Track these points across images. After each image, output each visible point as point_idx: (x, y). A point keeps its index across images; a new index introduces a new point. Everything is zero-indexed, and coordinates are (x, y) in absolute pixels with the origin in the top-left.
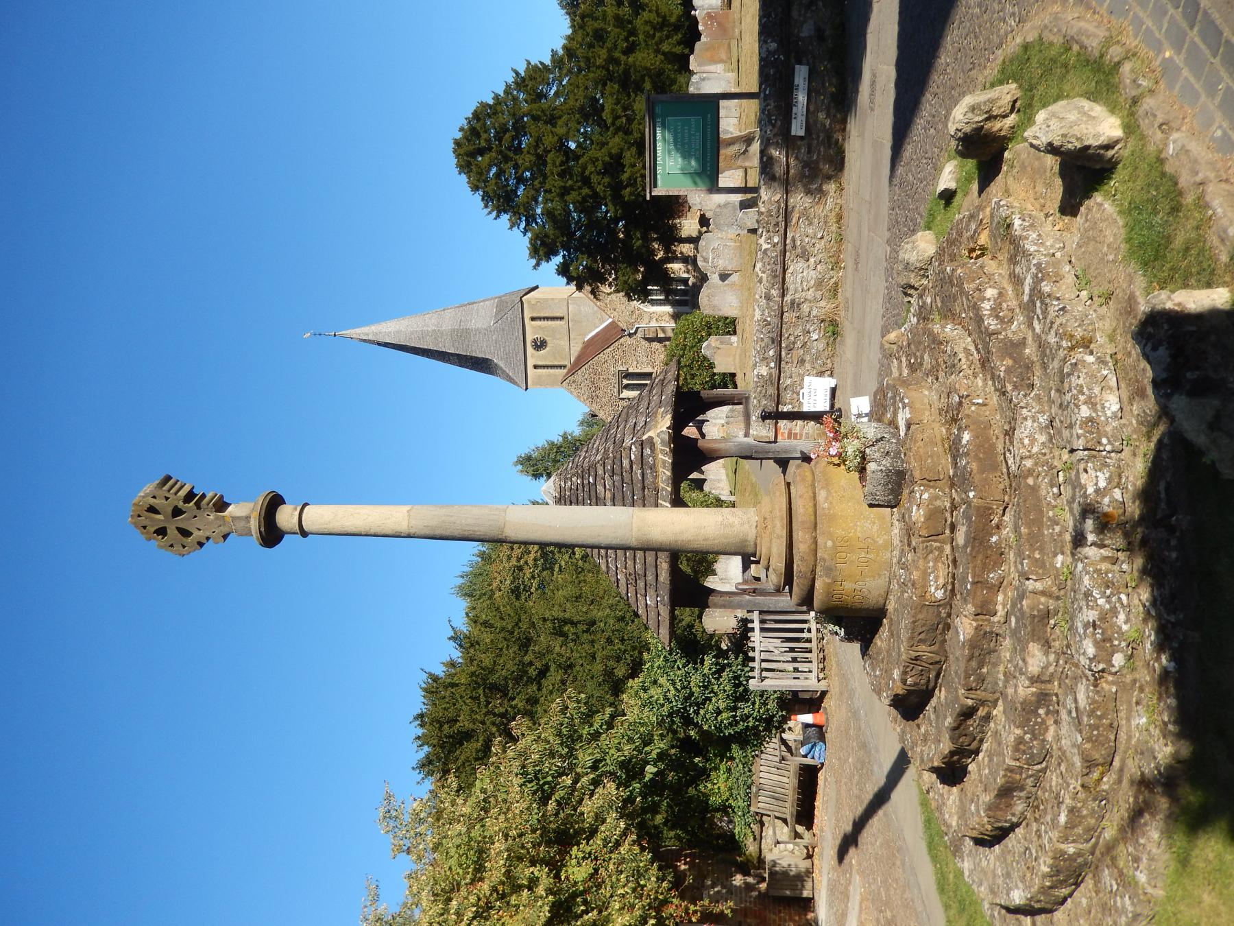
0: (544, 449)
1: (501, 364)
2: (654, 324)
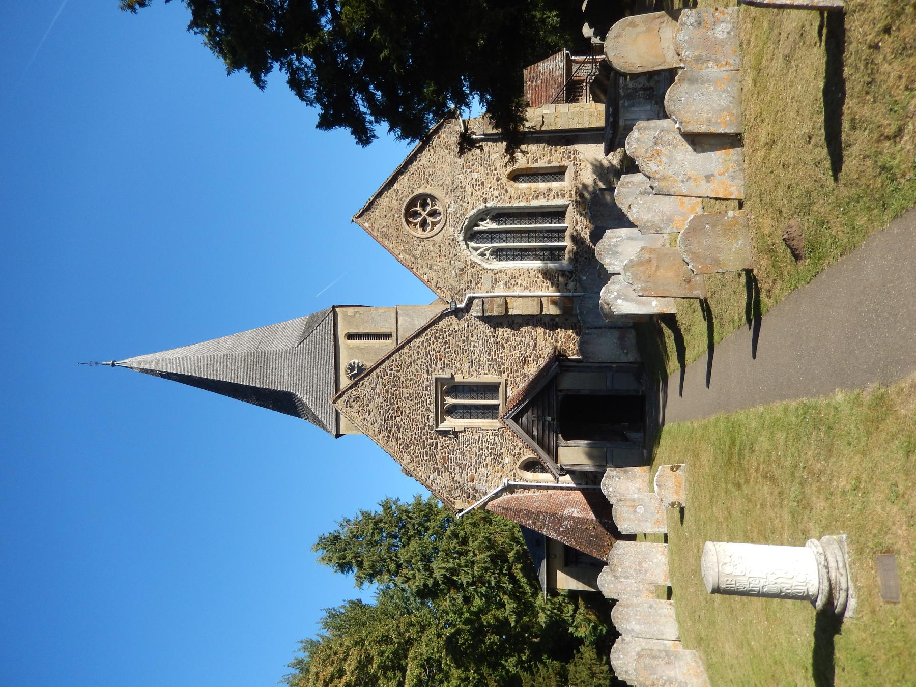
0: (357, 523)
1: (306, 400)
2: (500, 291)
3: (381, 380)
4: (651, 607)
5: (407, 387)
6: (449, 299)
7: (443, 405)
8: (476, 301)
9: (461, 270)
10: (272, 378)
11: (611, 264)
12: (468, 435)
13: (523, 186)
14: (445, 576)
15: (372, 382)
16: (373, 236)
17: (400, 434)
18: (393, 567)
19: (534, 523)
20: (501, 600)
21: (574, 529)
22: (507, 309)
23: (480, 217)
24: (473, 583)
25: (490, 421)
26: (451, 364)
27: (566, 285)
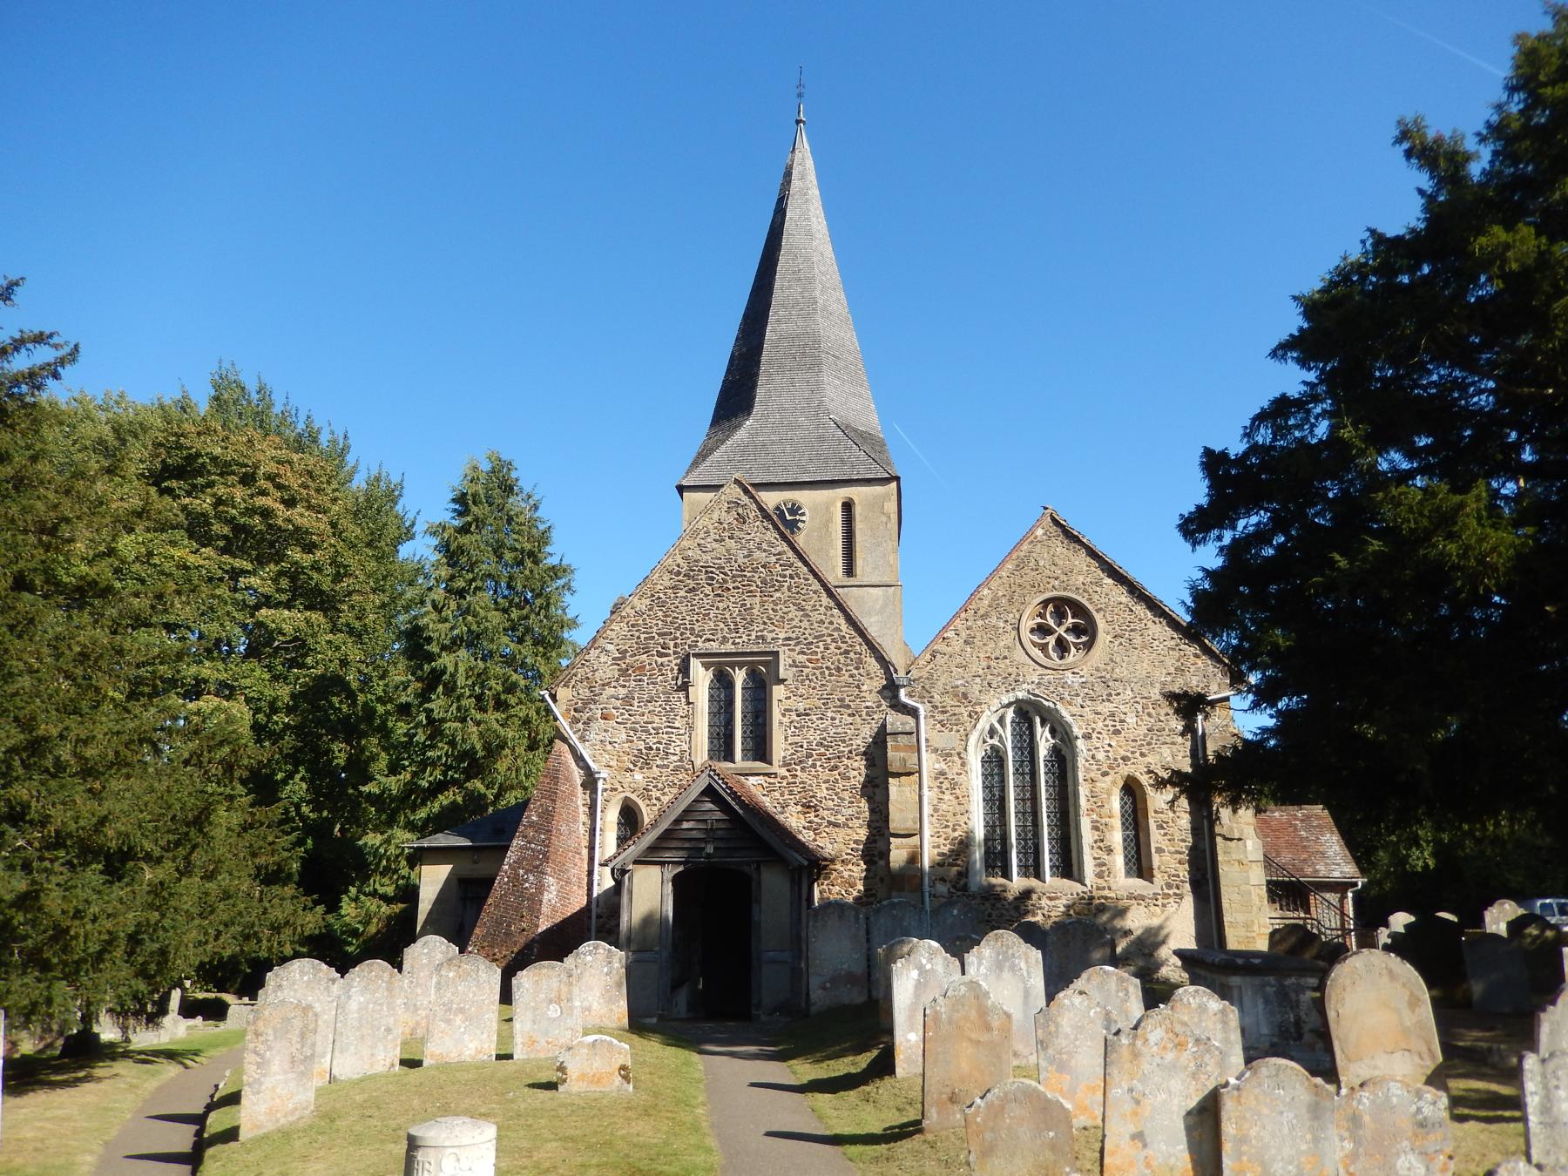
0: (532, 523)
1: (741, 435)
2: (930, 763)
3: (773, 559)
4: (388, 1030)
5: (762, 603)
6: (914, 674)
7: (733, 665)
8: (911, 721)
9: (965, 696)
10: (777, 378)
11: (980, 959)
12: (682, 708)
13: (1115, 803)
14: (444, 672)
15: (770, 544)
16: (1020, 543)
17: (682, 593)
18: (460, 583)
19: (532, 825)
20: (404, 768)
21: (521, 894)
22: (898, 775)
23: (1059, 728)
24: (431, 721)
25: (706, 748)
26: (802, 679)
27: (943, 880)
